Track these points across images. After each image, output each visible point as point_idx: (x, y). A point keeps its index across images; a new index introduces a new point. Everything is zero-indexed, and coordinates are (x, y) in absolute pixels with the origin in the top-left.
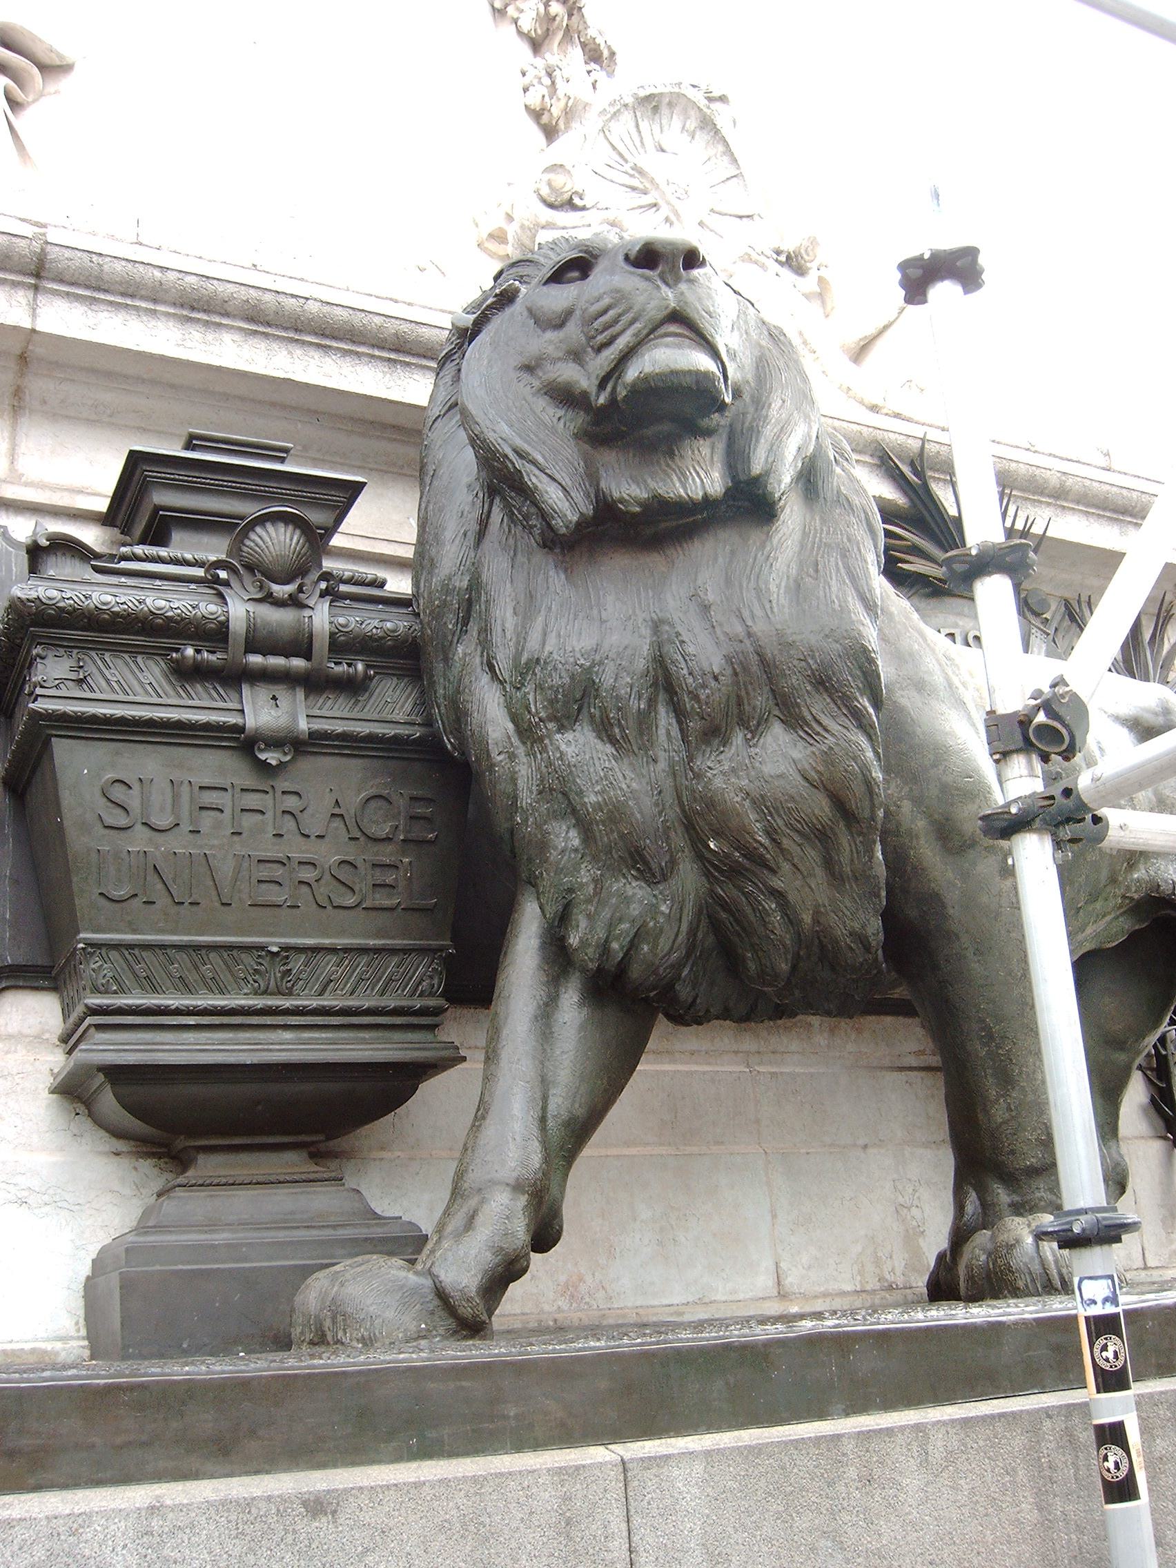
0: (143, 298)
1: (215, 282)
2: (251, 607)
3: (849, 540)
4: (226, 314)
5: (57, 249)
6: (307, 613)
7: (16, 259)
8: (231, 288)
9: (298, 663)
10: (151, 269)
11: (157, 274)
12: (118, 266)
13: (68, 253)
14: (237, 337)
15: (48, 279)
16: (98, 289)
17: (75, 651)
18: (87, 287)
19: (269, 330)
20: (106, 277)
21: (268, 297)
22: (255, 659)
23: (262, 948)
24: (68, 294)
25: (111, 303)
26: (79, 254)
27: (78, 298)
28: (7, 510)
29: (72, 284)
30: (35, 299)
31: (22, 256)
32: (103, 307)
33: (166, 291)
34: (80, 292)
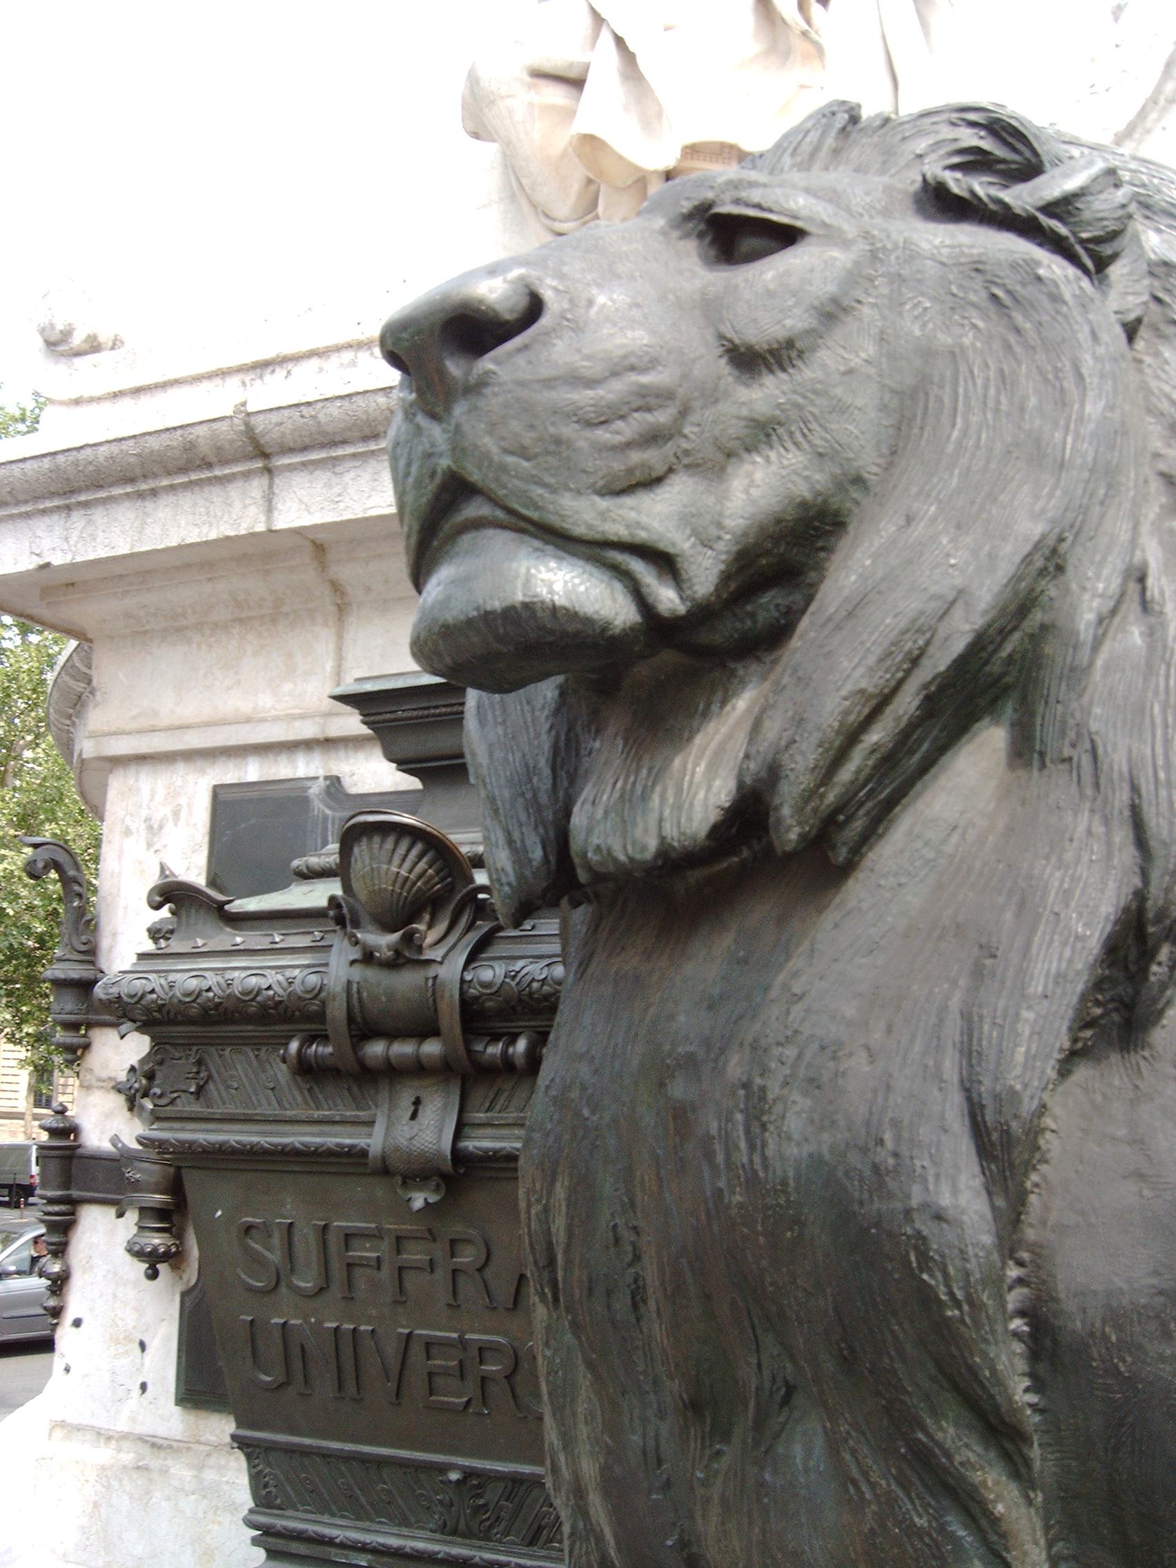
2: (357, 973)
3: (1022, 904)
5: (261, 417)
7: (227, 446)
9: (432, 1048)
10: (371, 397)
11: (382, 400)
12: (334, 410)
13: (275, 418)
15: (278, 454)
16: (334, 444)
17: (195, 1048)
18: (322, 446)
20: (329, 429)
22: (376, 1049)
23: (443, 1469)
24: (304, 464)
25: (354, 456)
26: (286, 413)
27: (317, 464)
28: (346, 747)
29: (305, 449)
30: (271, 486)
31: (232, 442)
32: (349, 464)
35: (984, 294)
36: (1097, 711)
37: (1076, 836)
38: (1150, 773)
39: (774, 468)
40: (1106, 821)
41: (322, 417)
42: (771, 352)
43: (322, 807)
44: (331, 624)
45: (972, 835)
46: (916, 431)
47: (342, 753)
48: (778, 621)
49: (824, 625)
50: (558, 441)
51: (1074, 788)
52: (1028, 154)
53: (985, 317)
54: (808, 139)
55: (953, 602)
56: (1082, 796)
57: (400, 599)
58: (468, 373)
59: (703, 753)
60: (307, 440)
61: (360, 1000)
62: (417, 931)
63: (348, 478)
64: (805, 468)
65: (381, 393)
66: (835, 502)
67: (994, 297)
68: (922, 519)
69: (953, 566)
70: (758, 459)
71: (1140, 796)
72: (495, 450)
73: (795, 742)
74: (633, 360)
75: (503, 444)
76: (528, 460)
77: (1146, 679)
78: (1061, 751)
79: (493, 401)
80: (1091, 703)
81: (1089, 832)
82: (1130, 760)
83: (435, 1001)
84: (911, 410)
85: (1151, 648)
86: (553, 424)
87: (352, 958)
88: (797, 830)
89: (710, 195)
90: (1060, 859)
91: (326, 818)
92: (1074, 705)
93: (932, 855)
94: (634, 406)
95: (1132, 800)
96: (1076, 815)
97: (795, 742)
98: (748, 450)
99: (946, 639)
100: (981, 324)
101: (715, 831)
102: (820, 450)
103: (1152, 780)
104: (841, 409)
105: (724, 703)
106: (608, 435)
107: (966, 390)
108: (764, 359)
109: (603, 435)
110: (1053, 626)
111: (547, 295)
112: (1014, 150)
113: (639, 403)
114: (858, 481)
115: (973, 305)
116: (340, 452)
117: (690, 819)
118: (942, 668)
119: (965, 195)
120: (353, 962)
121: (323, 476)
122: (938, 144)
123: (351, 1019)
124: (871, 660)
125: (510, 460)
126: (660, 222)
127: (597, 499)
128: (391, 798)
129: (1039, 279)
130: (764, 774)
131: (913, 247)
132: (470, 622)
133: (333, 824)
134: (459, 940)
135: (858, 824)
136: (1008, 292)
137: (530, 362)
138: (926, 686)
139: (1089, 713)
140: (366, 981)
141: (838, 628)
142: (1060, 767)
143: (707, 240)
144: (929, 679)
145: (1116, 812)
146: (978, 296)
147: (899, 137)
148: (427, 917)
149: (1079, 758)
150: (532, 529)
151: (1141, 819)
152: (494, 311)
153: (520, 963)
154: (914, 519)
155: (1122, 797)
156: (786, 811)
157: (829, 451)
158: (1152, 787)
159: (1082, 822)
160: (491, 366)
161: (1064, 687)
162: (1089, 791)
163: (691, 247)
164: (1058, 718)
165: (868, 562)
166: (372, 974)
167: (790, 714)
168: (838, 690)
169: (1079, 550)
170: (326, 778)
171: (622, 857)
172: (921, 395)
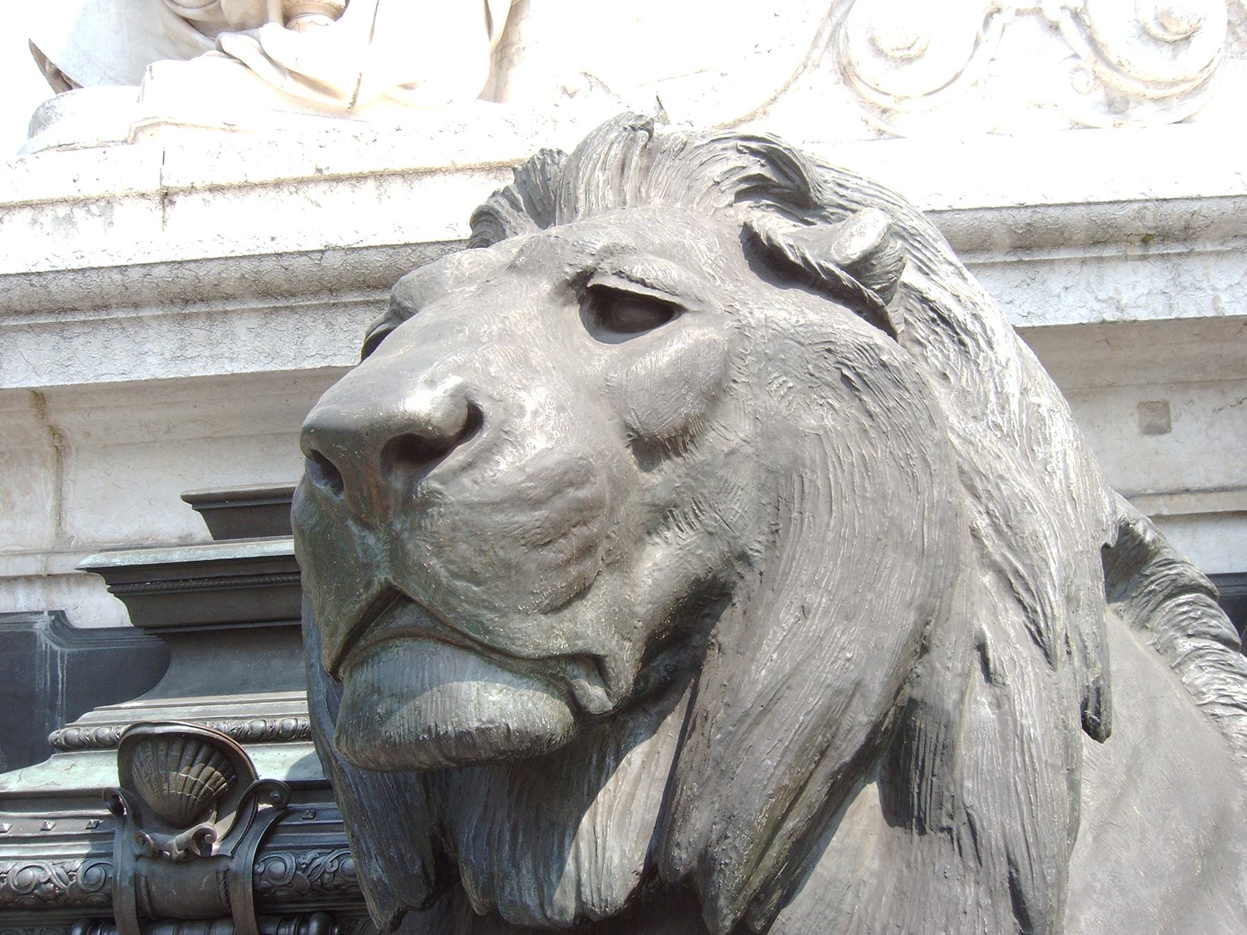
0: (120, 306)
1: (192, 266)
2: (143, 867)
4: (228, 298)
6: (222, 865)
8: (215, 268)
11: (117, 277)
14: (254, 322)
16: (62, 310)
18: (51, 312)
19: (292, 302)
20: (60, 298)
21: (268, 265)
24: (30, 326)
25: (84, 322)
26: (14, 280)
27: (44, 327)
33: (139, 293)
34: (42, 320)
35: (837, 375)
36: (968, 784)
37: (968, 910)
38: (1024, 849)
39: (672, 549)
40: (991, 893)
41: (52, 287)
42: (669, 440)
43: (49, 642)
44: (49, 464)
45: (865, 893)
46: (795, 514)
47: (64, 586)
48: (665, 679)
49: (740, 721)
50: (507, 566)
51: (957, 858)
52: (798, 181)
53: (839, 398)
54: (612, 153)
55: (853, 695)
56: (966, 867)
57: (120, 445)
58: (411, 489)
59: (610, 813)
60: (35, 306)
61: (149, 892)
62: (207, 831)
63: (78, 342)
64: (698, 547)
65: (115, 271)
66: (723, 576)
67: (845, 379)
68: (817, 610)
69: (848, 660)
70: (657, 540)
71: (1017, 871)
72: (443, 572)
73: (727, 837)
74: (571, 476)
75: (451, 567)
76: (478, 584)
77: (1004, 755)
78: (939, 820)
79: (438, 521)
80: (962, 779)
81: (978, 904)
82: (1004, 836)
83: (227, 894)
84: (783, 490)
85: (1002, 720)
86: (502, 548)
87: (138, 852)
88: (731, 917)
89: (590, 262)
90: (958, 929)
91: (54, 654)
92: (948, 779)
93: (832, 915)
94: (573, 522)
95: (1010, 873)
96: (963, 885)
97: (727, 837)
98: (649, 533)
99: (849, 731)
100: (836, 405)
101: (635, 897)
102: (710, 529)
103: (1026, 855)
104: (725, 488)
105: (618, 760)
106: (552, 555)
107: (835, 476)
108: (664, 446)
109: (549, 555)
110: (923, 702)
111: (484, 405)
112: (787, 177)
113: (578, 518)
114: (744, 557)
115: (828, 385)
116: (69, 319)
117: (610, 887)
118: (848, 759)
119: (799, 262)
120: (138, 857)
121: (50, 340)
122: (731, 171)
123: (139, 908)
124: (789, 759)
125: (459, 584)
126: (546, 286)
127: (543, 617)
128: (120, 634)
129: (884, 365)
130: (695, 863)
131: (775, 326)
132: (419, 743)
133: (62, 662)
134: (245, 835)
135: (775, 898)
136: (858, 375)
137: (475, 482)
138: (834, 775)
139: (962, 786)
140: (154, 874)
141: (756, 723)
142: (939, 834)
143: (586, 306)
144: (836, 768)
145: (998, 885)
146: (833, 377)
147: (698, 162)
148: (215, 813)
149: (959, 833)
150: (479, 648)
151: (1020, 891)
152: (439, 429)
153: (311, 855)
154: (809, 613)
155: (1002, 869)
156: (722, 902)
157: (718, 530)
158: (1027, 862)
159: (969, 893)
160: (436, 485)
161: (938, 762)
162: (972, 864)
163: (573, 313)
164: (934, 790)
165: (775, 656)
166: (159, 868)
167: (717, 806)
168: (765, 787)
169: (939, 631)
170: (51, 613)
171: (538, 915)
172: (795, 477)
